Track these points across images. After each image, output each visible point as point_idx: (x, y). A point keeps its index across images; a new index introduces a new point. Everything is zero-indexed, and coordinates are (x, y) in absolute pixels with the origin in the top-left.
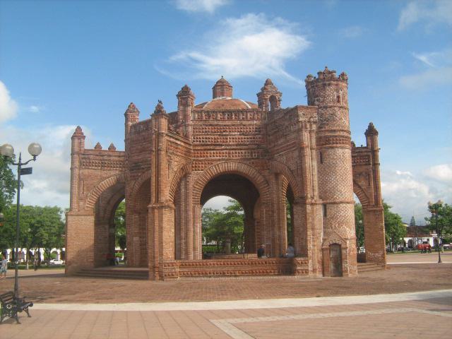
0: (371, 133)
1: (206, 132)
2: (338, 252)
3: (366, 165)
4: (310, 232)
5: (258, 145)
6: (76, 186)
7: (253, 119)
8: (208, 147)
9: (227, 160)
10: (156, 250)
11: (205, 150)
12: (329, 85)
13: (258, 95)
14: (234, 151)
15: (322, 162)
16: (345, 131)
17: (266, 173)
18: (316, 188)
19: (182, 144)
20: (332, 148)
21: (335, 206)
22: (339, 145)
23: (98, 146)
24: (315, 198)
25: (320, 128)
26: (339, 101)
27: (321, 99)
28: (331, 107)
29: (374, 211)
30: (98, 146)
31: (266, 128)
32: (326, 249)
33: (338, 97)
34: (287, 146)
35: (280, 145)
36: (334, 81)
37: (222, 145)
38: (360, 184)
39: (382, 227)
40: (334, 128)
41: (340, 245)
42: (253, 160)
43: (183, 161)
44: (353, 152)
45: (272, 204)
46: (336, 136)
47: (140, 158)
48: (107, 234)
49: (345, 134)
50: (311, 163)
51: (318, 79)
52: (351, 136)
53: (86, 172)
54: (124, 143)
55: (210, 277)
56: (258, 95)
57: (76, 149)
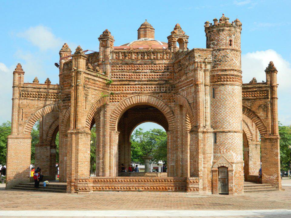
0: (271, 70)
1: (122, 69)
2: (226, 173)
3: (265, 98)
4: (201, 156)
5: (166, 81)
6: (16, 114)
7: (162, 59)
8: (124, 83)
9: (139, 93)
10: (73, 168)
11: (121, 85)
12: (223, 30)
13: (168, 38)
14: (145, 86)
15: (214, 97)
16: (235, 70)
17: (172, 104)
18: (209, 119)
19: (101, 80)
20: (223, 85)
21: (224, 134)
22: (228, 83)
23: (36, 81)
24: (207, 127)
25: (214, 67)
26: (230, 45)
27: (216, 43)
28: (223, 50)
29: (270, 139)
30: (36, 81)
31: (174, 66)
32: (216, 171)
33: (231, 41)
34: (187, 82)
35: (183, 81)
36: (227, 27)
37: (135, 81)
38: (259, 115)
39: (277, 153)
40: (226, 68)
41: (227, 168)
42: (161, 94)
43: (101, 95)
44: (243, 88)
45: (177, 132)
46: (227, 75)
48: (49, 154)
49: (236, 73)
50: (204, 97)
51: (214, 25)
52: (242, 75)
53: (25, 102)
54: (59, 77)
55: (118, 191)
56: (168, 38)
57: (17, 83)
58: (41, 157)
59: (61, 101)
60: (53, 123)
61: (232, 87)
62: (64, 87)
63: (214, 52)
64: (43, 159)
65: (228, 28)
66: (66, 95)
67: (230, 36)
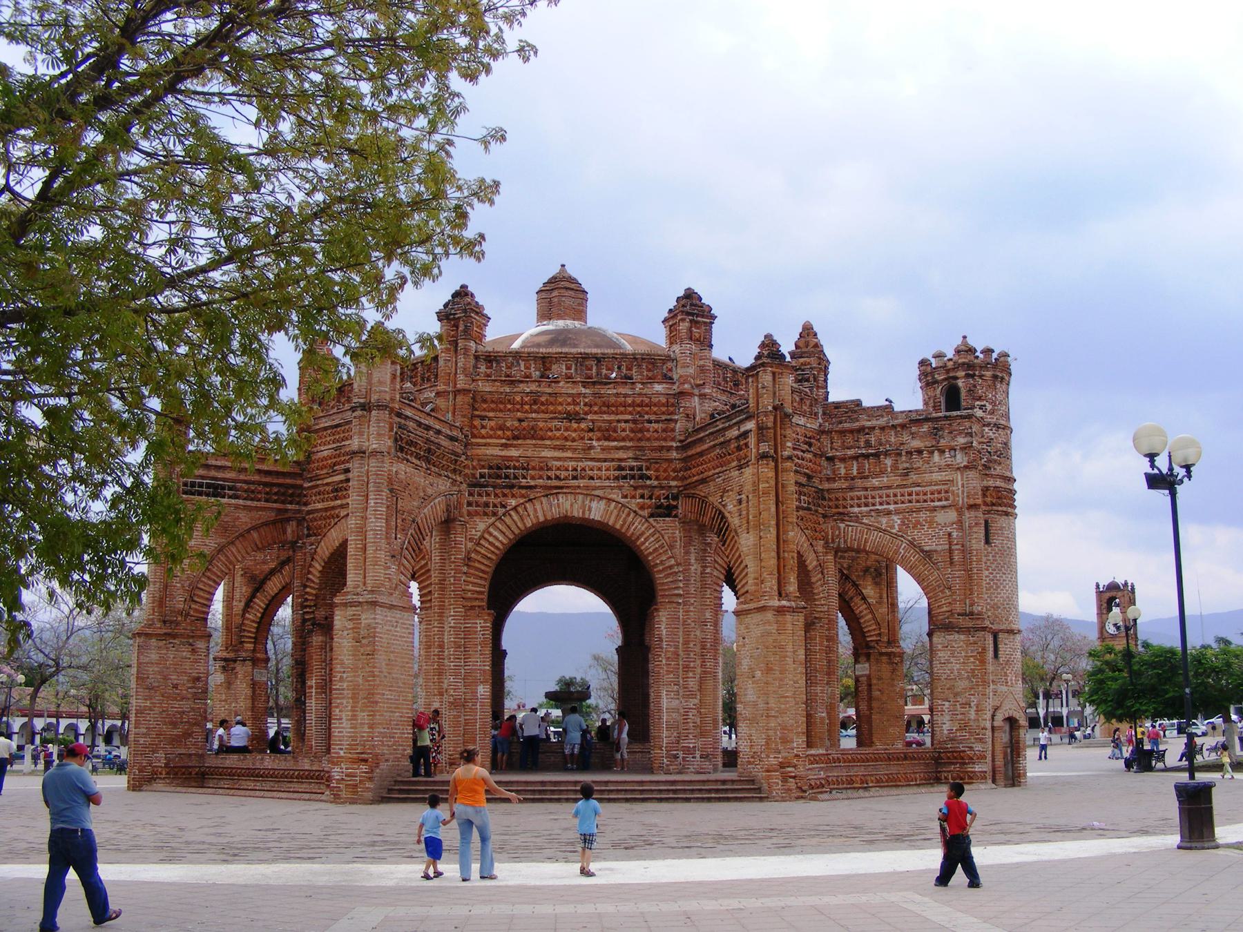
27: (989, 407)
47: (514, 453)
58: (166, 678)
59: (464, 486)
60: (220, 550)
62: (474, 436)
63: (986, 429)
64: (175, 686)
66: (490, 468)
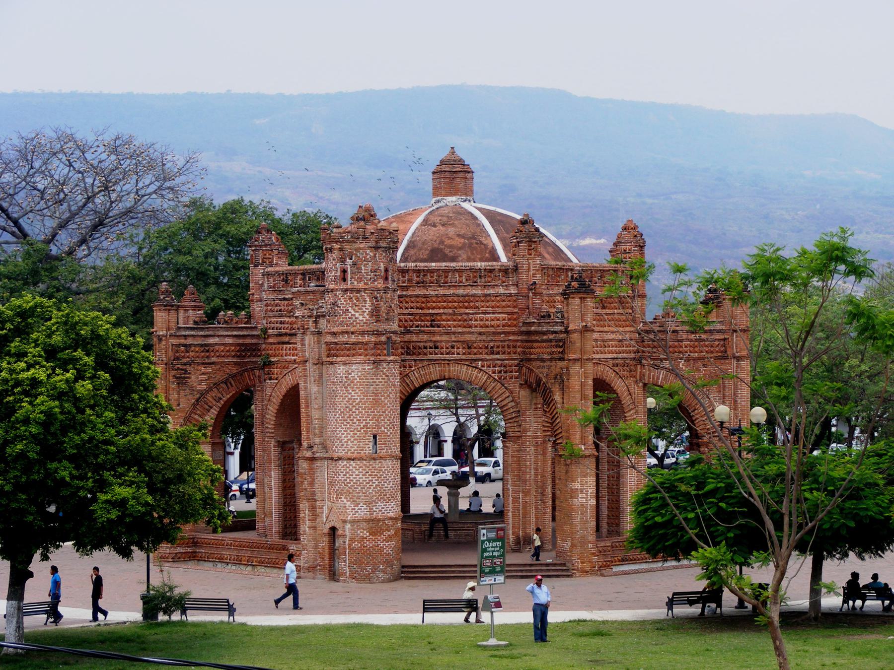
1: (280, 311)
11: (279, 343)
22: (339, 359)
24: (315, 449)
26: (344, 280)
28: (332, 291)
33: (344, 271)
61: (347, 368)
65: (336, 246)
67: (343, 261)
